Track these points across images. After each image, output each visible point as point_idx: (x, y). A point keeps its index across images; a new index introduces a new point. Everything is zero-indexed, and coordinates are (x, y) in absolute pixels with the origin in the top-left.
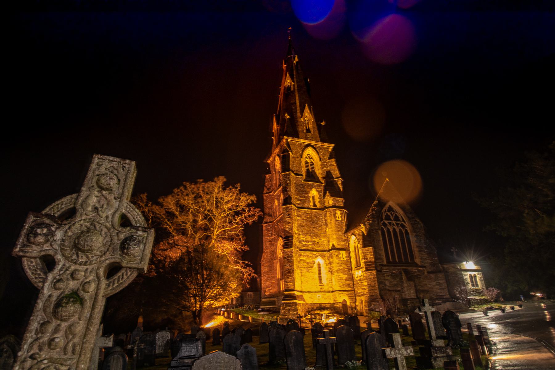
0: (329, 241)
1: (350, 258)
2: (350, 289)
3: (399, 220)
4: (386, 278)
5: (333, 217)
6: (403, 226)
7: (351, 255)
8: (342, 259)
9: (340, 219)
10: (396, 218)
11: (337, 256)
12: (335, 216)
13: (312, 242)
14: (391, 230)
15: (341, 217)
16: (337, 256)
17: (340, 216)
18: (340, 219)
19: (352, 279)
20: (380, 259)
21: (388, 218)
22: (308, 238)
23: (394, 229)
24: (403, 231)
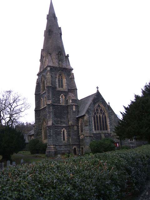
0: (69, 121)
2: (77, 143)
3: (102, 111)
6: (104, 114)
7: (79, 127)
8: (75, 129)
9: (75, 110)
10: (101, 110)
12: (72, 109)
13: (61, 121)
14: (98, 116)
18: (75, 110)
19: (79, 139)
20: (92, 130)
21: (97, 110)
22: (59, 119)
23: (100, 115)
24: (104, 116)
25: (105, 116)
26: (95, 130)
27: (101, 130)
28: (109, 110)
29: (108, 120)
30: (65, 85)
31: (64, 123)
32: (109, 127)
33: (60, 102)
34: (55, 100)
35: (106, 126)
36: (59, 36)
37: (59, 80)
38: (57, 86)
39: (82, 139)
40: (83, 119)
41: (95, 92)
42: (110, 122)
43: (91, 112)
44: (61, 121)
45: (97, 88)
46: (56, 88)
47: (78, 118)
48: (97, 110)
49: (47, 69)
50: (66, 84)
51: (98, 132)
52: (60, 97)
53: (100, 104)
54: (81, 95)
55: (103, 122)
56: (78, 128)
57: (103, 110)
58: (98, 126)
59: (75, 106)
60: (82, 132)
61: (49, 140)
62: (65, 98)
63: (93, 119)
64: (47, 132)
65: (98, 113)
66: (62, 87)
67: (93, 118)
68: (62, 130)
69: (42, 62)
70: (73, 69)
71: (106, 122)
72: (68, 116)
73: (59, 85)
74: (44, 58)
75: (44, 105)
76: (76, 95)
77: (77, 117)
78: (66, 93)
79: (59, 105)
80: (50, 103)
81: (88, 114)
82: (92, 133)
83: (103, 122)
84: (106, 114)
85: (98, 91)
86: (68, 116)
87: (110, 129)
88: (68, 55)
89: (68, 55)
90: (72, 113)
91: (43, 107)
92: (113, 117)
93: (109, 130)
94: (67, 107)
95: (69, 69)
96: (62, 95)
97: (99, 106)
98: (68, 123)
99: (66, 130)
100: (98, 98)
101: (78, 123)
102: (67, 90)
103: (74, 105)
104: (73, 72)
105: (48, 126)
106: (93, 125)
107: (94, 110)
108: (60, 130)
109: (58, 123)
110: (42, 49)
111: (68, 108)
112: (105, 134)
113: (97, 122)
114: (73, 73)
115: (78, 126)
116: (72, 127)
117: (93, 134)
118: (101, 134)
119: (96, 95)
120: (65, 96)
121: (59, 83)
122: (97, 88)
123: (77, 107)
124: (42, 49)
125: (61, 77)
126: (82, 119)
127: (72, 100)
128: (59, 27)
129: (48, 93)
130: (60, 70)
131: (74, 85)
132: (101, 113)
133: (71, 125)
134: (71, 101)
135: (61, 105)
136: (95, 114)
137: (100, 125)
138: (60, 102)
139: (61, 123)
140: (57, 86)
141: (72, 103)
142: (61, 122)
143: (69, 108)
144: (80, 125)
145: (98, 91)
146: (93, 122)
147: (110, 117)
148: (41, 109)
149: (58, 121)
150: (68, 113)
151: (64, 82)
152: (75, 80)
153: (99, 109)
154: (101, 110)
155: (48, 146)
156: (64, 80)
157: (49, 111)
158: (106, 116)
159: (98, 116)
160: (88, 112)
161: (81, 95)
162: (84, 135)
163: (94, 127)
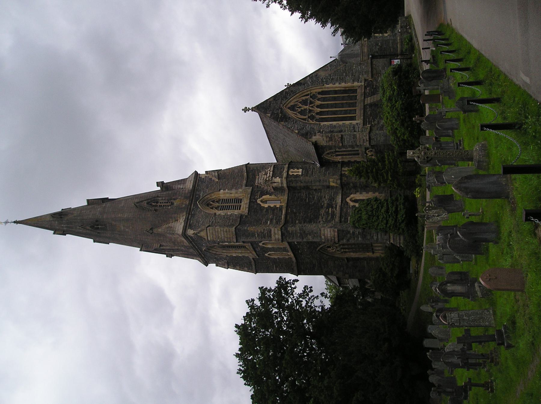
0: (328, 187)
1: (349, 162)
3: (307, 99)
4: (376, 122)
5: (298, 179)
6: (313, 97)
7: (346, 160)
9: (301, 170)
11: (347, 177)
12: (297, 176)
13: (328, 208)
14: (319, 110)
15: (298, 169)
16: (347, 177)
17: (296, 170)
18: (301, 170)
20: (354, 127)
21: (302, 113)
22: (322, 211)
25: (319, 93)
26: (353, 118)
27: (354, 105)
28: (304, 84)
29: (330, 86)
30: (233, 194)
31: (332, 199)
32: (349, 84)
33: (278, 206)
34: (271, 220)
35: (345, 91)
36: (109, 204)
37: (223, 208)
38: (236, 212)
39: (376, 152)
40: (323, 147)
41: (256, 116)
42: (337, 81)
43: (308, 128)
44: (328, 208)
45: (246, 110)
46: (241, 216)
47: (324, 163)
48: (302, 113)
49: (191, 237)
50: (234, 191)
51: (359, 112)
52: (266, 206)
53: (289, 105)
54: (263, 154)
55: (335, 99)
56: (348, 164)
57: (304, 98)
58: (346, 112)
59: (292, 170)
60: (358, 154)
61: (375, 238)
62: (267, 193)
63: (326, 123)
64: (353, 242)
65: (310, 111)
66: (240, 201)
67: (322, 124)
68: (352, 204)
69: (173, 250)
70: (196, 172)
71: (336, 92)
72: (314, 188)
73: (235, 208)
74: (163, 246)
75: (285, 250)
76: (262, 167)
77: (318, 165)
78: (256, 192)
79: (287, 210)
80: (280, 232)
81: (311, 133)
82: (361, 126)
83: (335, 99)
84: (316, 90)
85: (253, 109)
86: (316, 190)
87: (353, 81)
88: (158, 184)
89: (158, 184)
90: (307, 178)
91: (291, 254)
92: (322, 74)
93: (356, 84)
94: (293, 189)
95: (195, 182)
96: (261, 201)
97: (292, 108)
98: (333, 187)
99: (352, 196)
100: (274, 112)
101: (336, 163)
102: (249, 190)
103: (288, 172)
104: (202, 172)
105: (339, 241)
106: (341, 123)
107: (305, 119)
108: (350, 211)
109: (333, 214)
110: (141, 250)
111: (295, 188)
112: (365, 95)
113: (334, 113)
114: (206, 172)
115: (343, 164)
116: (344, 179)
117: (364, 124)
118: (366, 104)
119: (265, 113)
120: (263, 193)
121: (228, 208)
122: (246, 110)
123: (292, 165)
124: (139, 249)
125: (213, 201)
126: (323, 153)
127: (274, 175)
128: (86, 204)
129: (253, 235)
130: (196, 205)
131: (236, 171)
132: (311, 103)
133: (339, 182)
134: (278, 180)
135: (285, 206)
136: (312, 118)
137: (342, 105)
138: (278, 206)
139: (332, 207)
140: (236, 212)
141: (281, 177)
142: (330, 206)
143: (294, 185)
144: (339, 159)
145: (253, 109)
146: (334, 123)
147: (322, 81)
148: (294, 259)
149: (328, 213)
150: (307, 188)
151: (227, 196)
152: (223, 168)
153: (300, 107)
154: (305, 102)
155: (392, 241)
156: (223, 194)
157: (301, 234)
158: (320, 90)
159: (319, 110)
160: (306, 135)
161: (263, 154)
162: (366, 149)
163: (348, 122)
